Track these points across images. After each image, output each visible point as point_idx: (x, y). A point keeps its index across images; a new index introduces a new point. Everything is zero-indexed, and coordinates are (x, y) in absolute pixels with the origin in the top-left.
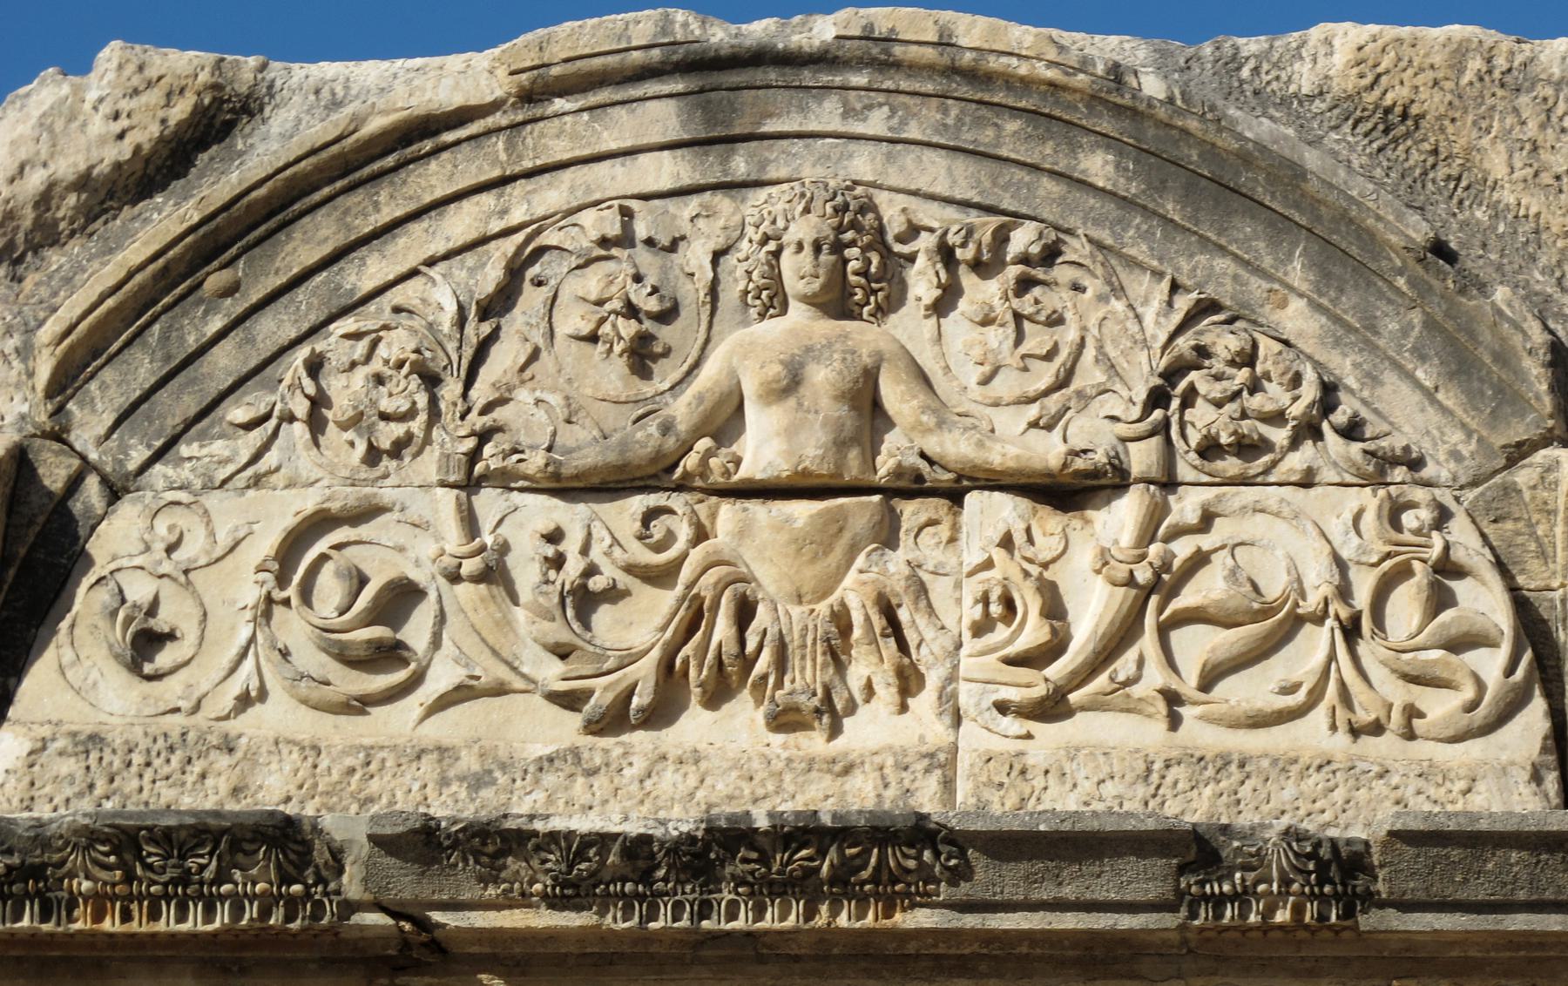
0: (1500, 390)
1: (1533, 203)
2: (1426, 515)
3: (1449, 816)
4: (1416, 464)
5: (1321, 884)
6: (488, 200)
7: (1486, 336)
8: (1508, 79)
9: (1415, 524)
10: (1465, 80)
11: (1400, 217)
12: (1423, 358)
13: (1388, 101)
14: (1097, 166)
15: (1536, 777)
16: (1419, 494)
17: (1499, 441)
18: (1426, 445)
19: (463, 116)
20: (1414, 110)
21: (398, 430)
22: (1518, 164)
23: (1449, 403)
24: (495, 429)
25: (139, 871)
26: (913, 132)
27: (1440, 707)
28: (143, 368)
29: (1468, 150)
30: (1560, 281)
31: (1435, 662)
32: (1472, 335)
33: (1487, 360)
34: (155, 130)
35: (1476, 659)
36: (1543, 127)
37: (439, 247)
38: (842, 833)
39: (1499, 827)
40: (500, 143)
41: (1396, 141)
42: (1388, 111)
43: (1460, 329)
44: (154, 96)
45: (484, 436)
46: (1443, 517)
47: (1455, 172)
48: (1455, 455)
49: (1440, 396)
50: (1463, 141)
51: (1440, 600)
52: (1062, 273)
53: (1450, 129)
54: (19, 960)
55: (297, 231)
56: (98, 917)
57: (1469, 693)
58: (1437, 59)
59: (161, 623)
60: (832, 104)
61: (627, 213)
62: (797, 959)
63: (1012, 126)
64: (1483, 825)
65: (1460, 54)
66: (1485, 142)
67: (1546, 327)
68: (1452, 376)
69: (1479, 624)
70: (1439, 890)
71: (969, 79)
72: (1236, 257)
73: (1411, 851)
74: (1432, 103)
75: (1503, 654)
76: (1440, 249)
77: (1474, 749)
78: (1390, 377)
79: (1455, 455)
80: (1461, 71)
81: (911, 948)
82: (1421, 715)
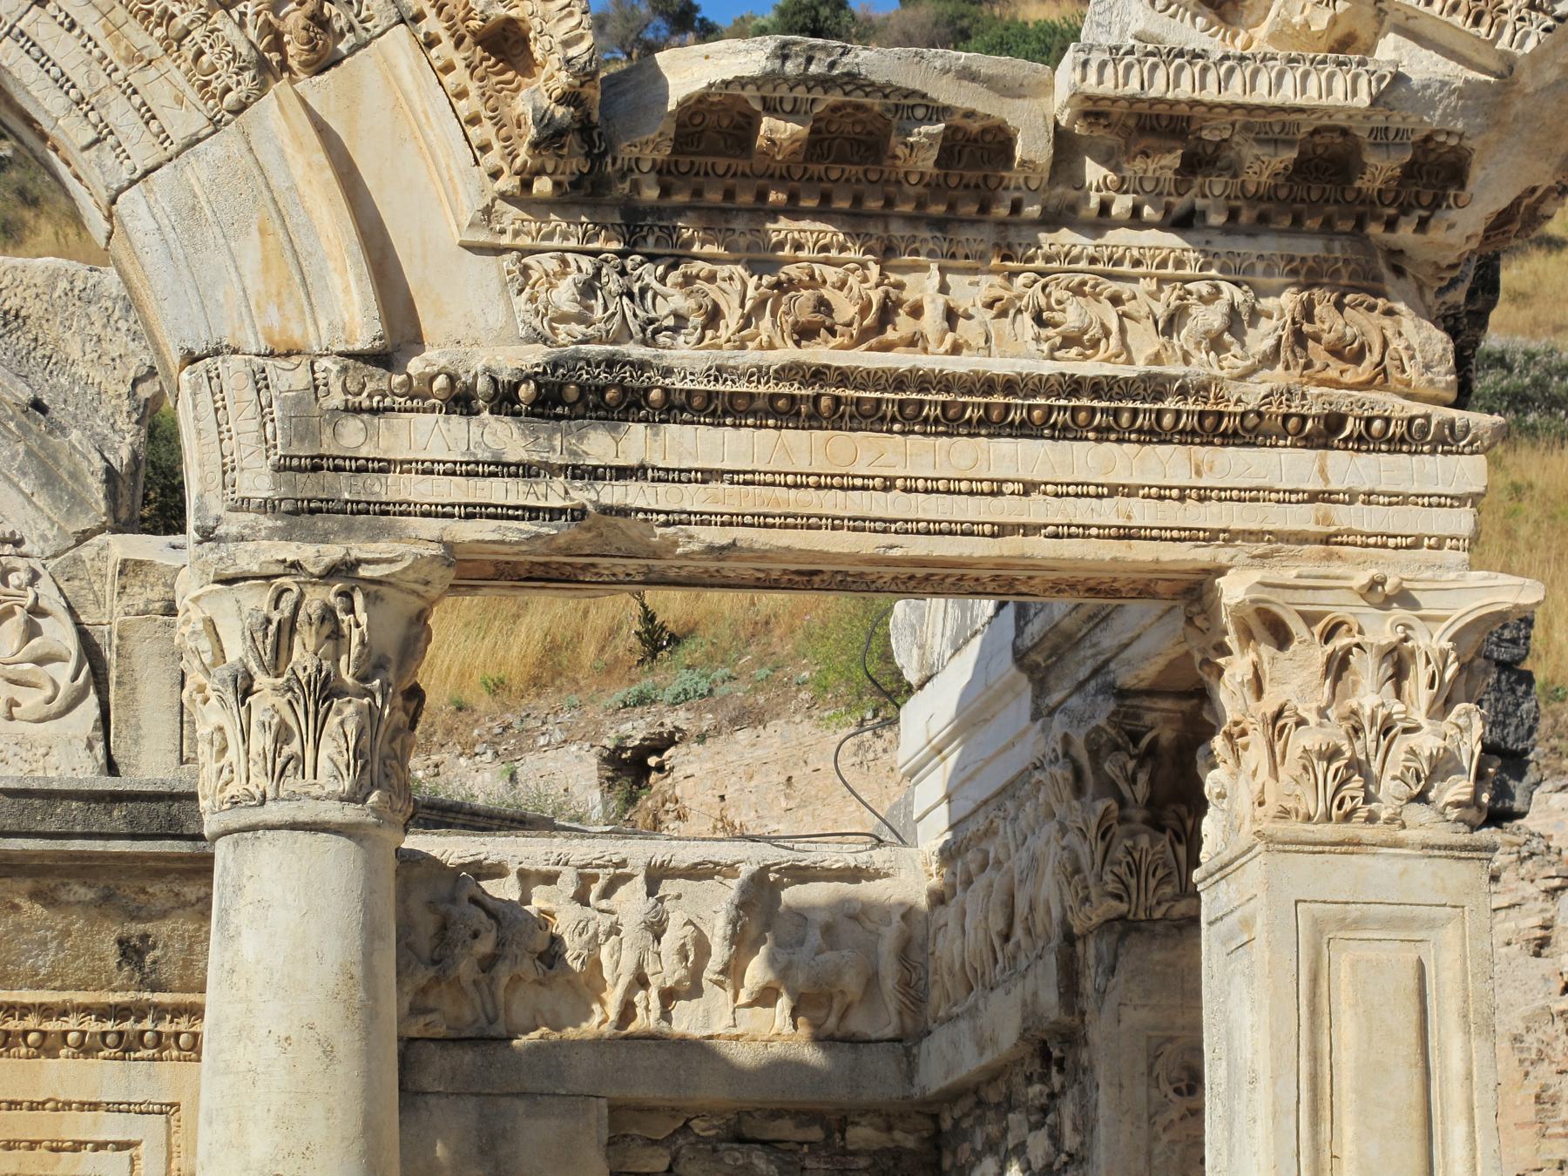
0: (73, 496)
1: (97, 376)
2: (24, 576)
3: (33, 779)
4: (18, 543)
7: (65, 462)
8: (83, 295)
9: (17, 582)
10: (56, 295)
11: (12, 384)
12: (25, 474)
13: (6, 307)
15: (90, 746)
16: (20, 563)
17: (71, 529)
18: (26, 533)
20: (23, 313)
22: (88, 350)
23: (40, 504)
27: (31, 700)
29: (57, 340)
30: (112, 426)
31: (28, 671)
32: (56, 461)
33: (66, 477)
35: (51, 668)
36: (105, 327)
39: (64, 787)
41: (11, 331)
42: (6, 313)
43: (49, 456)
46: (35, 576)
47: (48, 353)
48: (44, 538)
49: (34, 499)
50: (53, 334)
51: (32, 631)
53: (46, 326)
57: (49, 692)
58: (39, 281)
64: (55, 786)
65: (54, 277)
66: (68, 335)
67: (103, 457)
68: (42, 486)
69: (56, 649)
70: (27, 825)
73: (9, 801)
74: (34, 309)
75: (70, 667)
76: (38, 405)
77: (51, 726)
79: (44, 538)
80: (54, 289)
82: (18, 705)
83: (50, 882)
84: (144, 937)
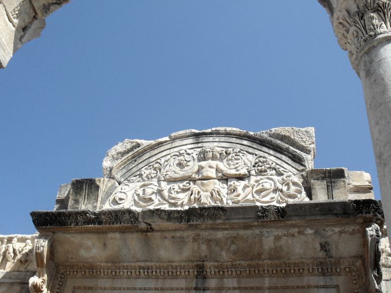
5: (278, 213)
6: (168, 150)
14: (245, 142)
19: (166, 142)
21: (155, 175)
24: (167, 174)
25: (112, 218)
26: (221, 140)
28: (125, 171)
34: (130, 147)
37: (162, 156)
38: (209, 208)
40: (170, 145)
44: (130, 143)
45: (167, 174)
52: (241, 155)
54: (96, 232)
55: (145, 155)
56: (106, 224)
59: (122, 198)
60: (212, 138)
61: (186, 151)
62: (202, 229)
63: (234, 139)
71: (228, 134)
72: (263, 152)
74: (288, 134)
78: (284, 163)
81: (219, 227)
83: (302, 229)
84: (326, 242)
